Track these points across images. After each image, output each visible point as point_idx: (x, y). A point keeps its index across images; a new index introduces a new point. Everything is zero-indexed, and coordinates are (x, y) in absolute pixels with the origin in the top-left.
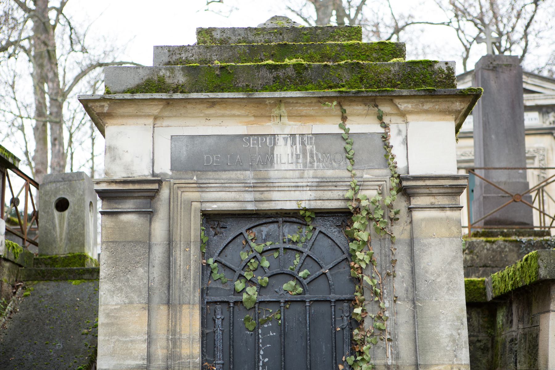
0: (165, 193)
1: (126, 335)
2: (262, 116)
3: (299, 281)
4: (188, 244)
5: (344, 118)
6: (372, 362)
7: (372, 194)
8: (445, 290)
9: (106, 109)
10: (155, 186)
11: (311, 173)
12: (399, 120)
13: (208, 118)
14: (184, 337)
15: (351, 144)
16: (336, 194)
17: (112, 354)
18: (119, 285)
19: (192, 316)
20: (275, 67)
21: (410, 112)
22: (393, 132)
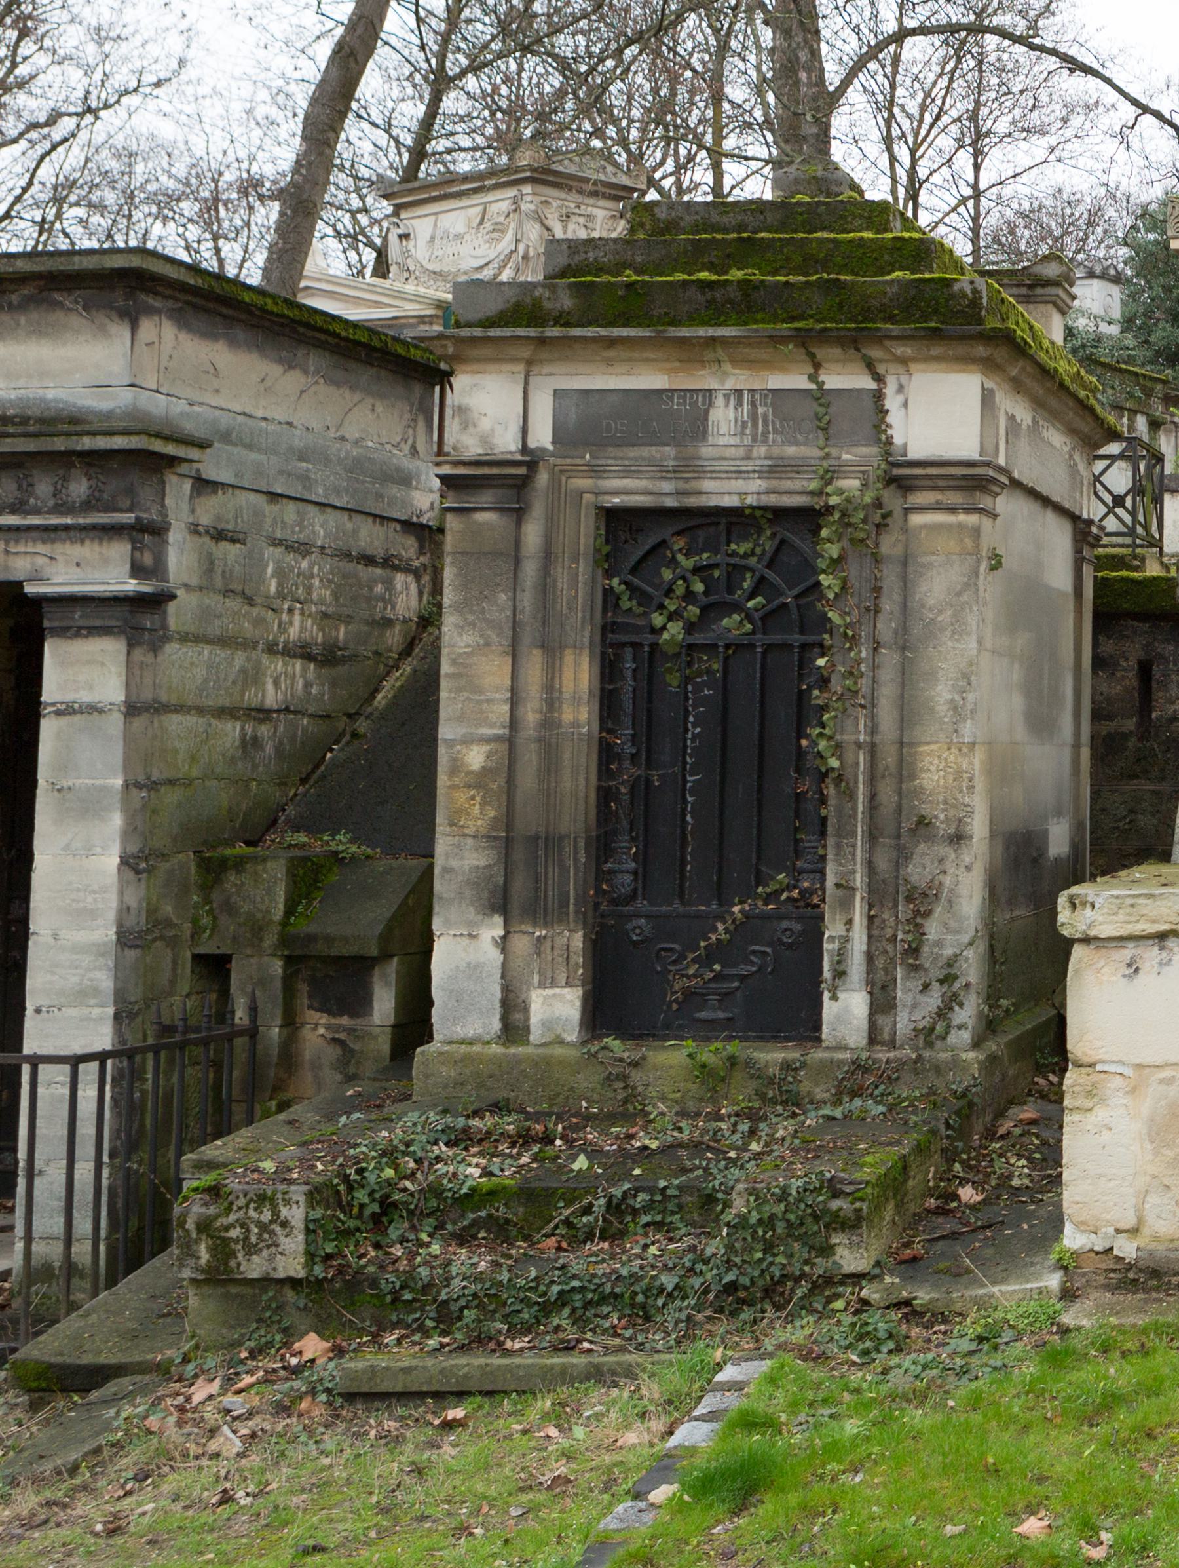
0: (543, 478)
1: (478, 690)
2: (689, 360)
3: (749, 617)
4: (575, 558)
5: (817, 366)
6: (838, 737)
7: (851, 484)
8: (948, 633)
9: (450, 350)
10: (522, 471)
11: (763, 450)
12: (901, 369)
13: (609, 362)
14: (566, 696)
15: (828, 405)
16: (797, 485)
17: (460, 718)
18: (470, 617)
19: (577, 664)
20: (710, 285)
21: (914, 360)
22: (890, 390)
